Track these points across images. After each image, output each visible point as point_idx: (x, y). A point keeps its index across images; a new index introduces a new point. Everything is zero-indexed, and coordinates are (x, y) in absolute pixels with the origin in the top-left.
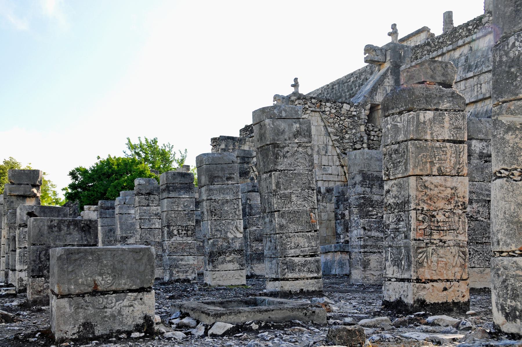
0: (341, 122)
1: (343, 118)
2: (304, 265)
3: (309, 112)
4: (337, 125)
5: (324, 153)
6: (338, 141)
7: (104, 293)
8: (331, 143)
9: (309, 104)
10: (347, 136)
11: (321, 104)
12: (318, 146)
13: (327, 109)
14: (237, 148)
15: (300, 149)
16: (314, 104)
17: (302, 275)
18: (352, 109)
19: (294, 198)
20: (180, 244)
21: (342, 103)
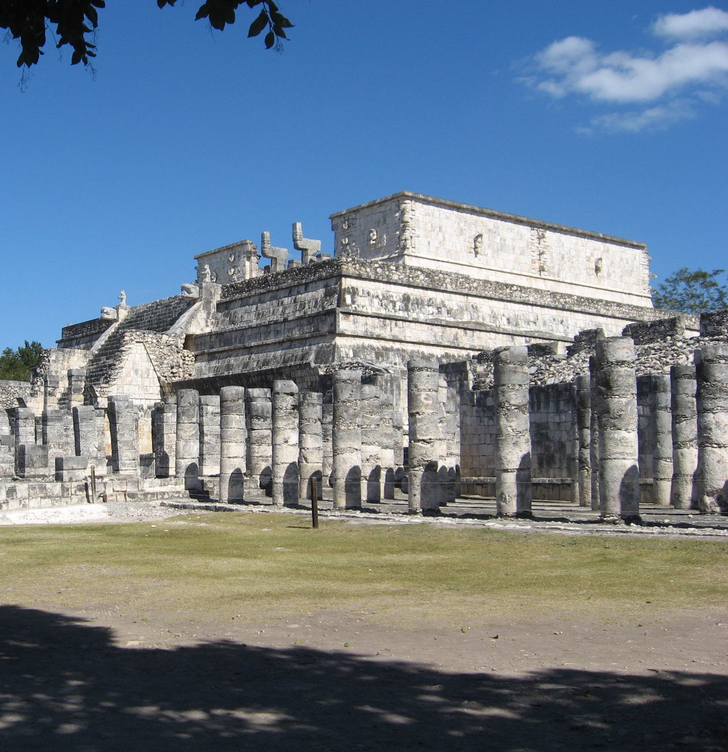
0: (161, 350)
1: (162, 347)
2: (130, 464)
3: (134, 342)
4: (157, 353)
5: (146, 376)
6: (158, 366)
7: (75, 469)
8: (152, 368)
9: (134, 336)
10: (166, 362)
12: (142, 371)
13: (150, 340)
14: (67, 359)
15: (128, 414)
16: (138, 336)
17: (129, 468)
18: (170, 339)
19: (126, 435)
20: (55, 453)
21: (162, 334)
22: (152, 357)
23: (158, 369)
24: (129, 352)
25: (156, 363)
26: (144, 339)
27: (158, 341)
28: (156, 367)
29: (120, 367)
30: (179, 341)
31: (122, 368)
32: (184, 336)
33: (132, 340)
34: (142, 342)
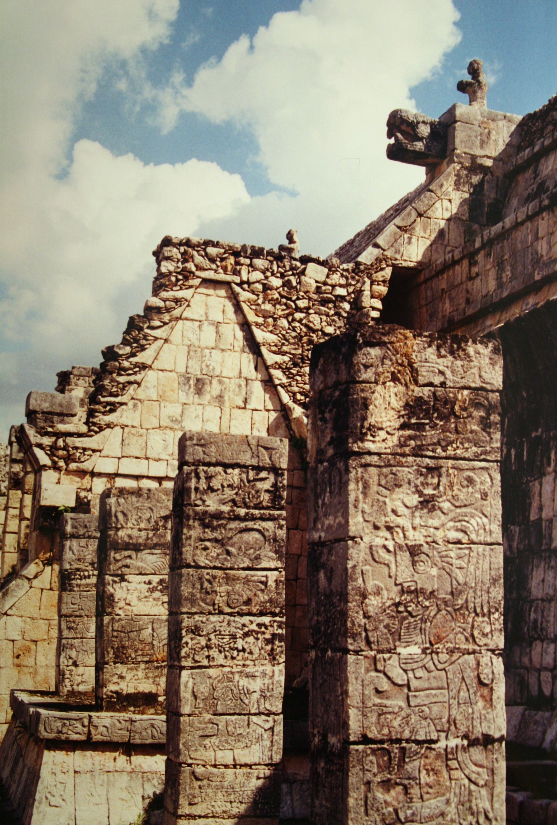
1: (302, 304)
6: (286, 370)
9: (198, 259)
11: (237, 263)
18: (336, 278)
22: (260, 335)
23: (285, 380)
24: (176, 313)
25: (279, 358)
26: (236, 273)
27: (287, 284)
28: (277, 374)
29: (136, 365)
30: (367, 293)
31: (143, 367)
32: (388, 272)
33: (187, 274)
34: (228, 284)
